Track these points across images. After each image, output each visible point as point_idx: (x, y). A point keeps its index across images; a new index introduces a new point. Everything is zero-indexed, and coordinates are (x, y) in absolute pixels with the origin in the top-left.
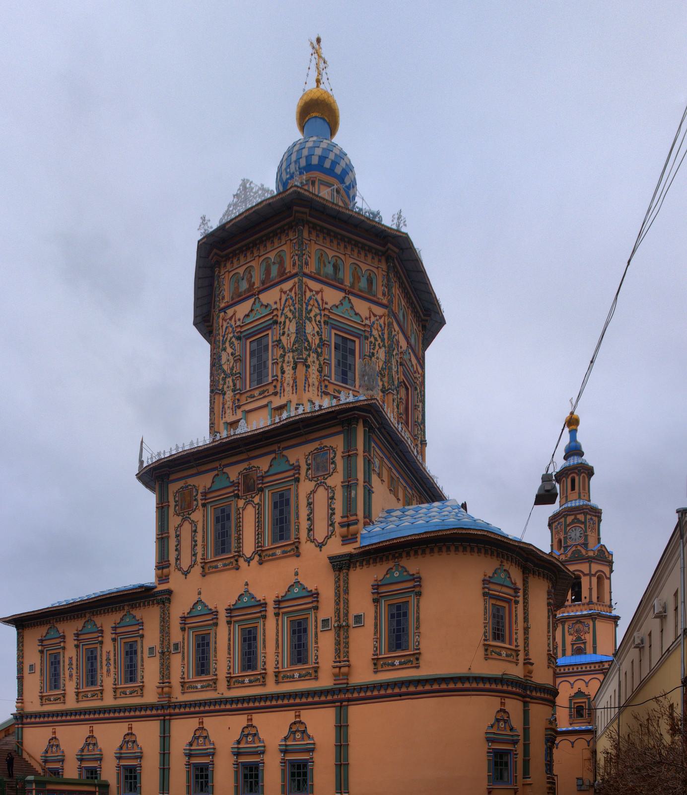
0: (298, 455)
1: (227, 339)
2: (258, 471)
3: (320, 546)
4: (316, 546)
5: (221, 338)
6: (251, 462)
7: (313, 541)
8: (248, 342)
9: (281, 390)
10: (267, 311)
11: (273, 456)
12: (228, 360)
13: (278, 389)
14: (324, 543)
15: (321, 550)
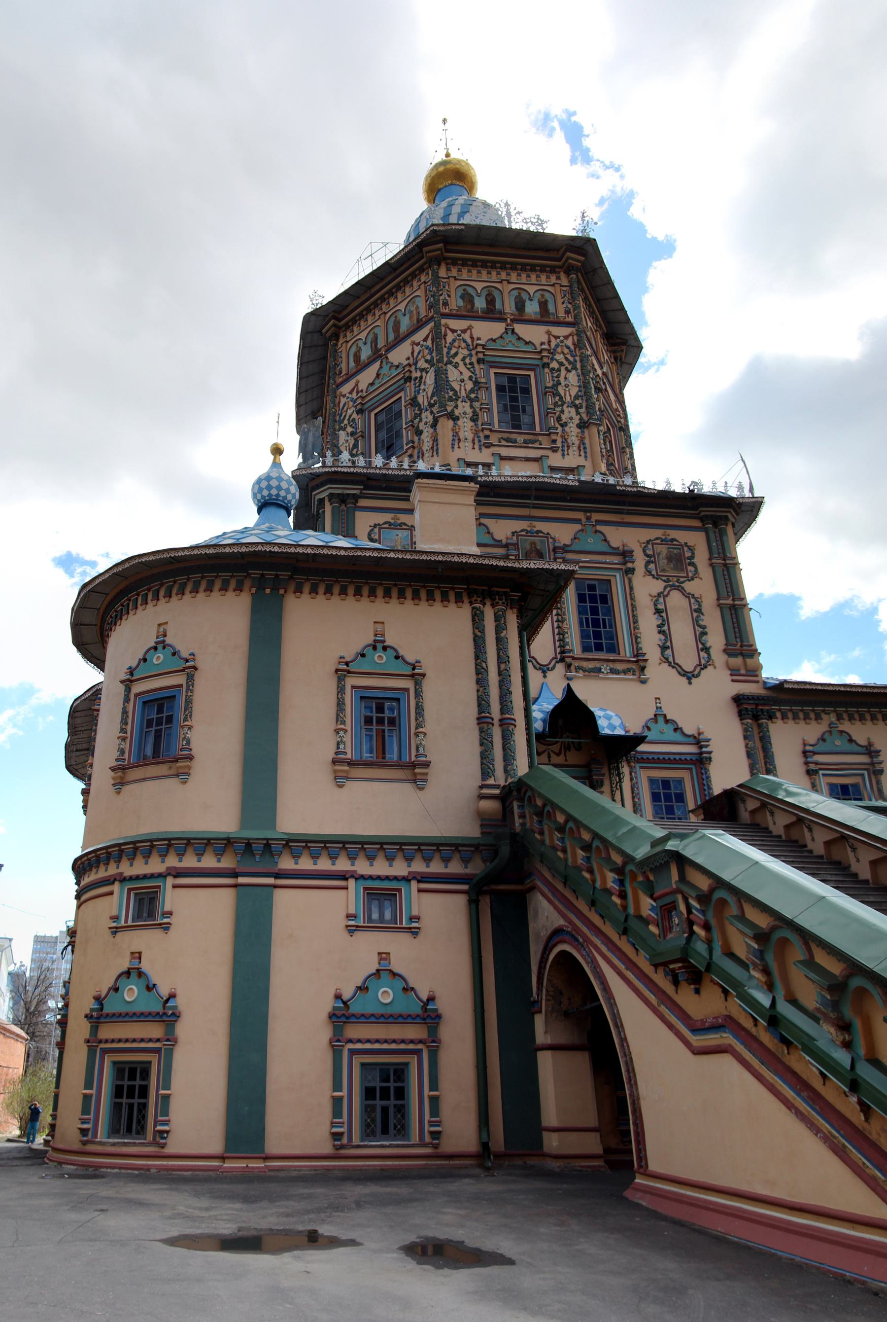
0: (629, 537)
1: (456, 354)
2: (550, 540)
3: (690, 676)
4: (679, 673)
5: (445, 350)
6: (535, 523)
7: (674, 665)
8: (492, 371)
9: (563, 446)
10: (399, 370)
11: (578, 527)
12: (462, 381)
13: (559, 444)
14: (696, 673)
15: (690, 683)
